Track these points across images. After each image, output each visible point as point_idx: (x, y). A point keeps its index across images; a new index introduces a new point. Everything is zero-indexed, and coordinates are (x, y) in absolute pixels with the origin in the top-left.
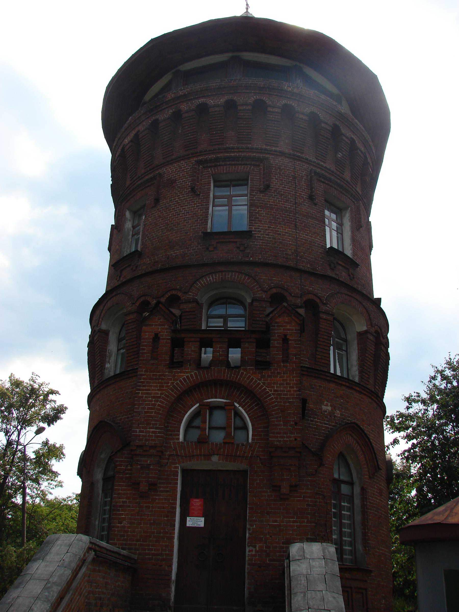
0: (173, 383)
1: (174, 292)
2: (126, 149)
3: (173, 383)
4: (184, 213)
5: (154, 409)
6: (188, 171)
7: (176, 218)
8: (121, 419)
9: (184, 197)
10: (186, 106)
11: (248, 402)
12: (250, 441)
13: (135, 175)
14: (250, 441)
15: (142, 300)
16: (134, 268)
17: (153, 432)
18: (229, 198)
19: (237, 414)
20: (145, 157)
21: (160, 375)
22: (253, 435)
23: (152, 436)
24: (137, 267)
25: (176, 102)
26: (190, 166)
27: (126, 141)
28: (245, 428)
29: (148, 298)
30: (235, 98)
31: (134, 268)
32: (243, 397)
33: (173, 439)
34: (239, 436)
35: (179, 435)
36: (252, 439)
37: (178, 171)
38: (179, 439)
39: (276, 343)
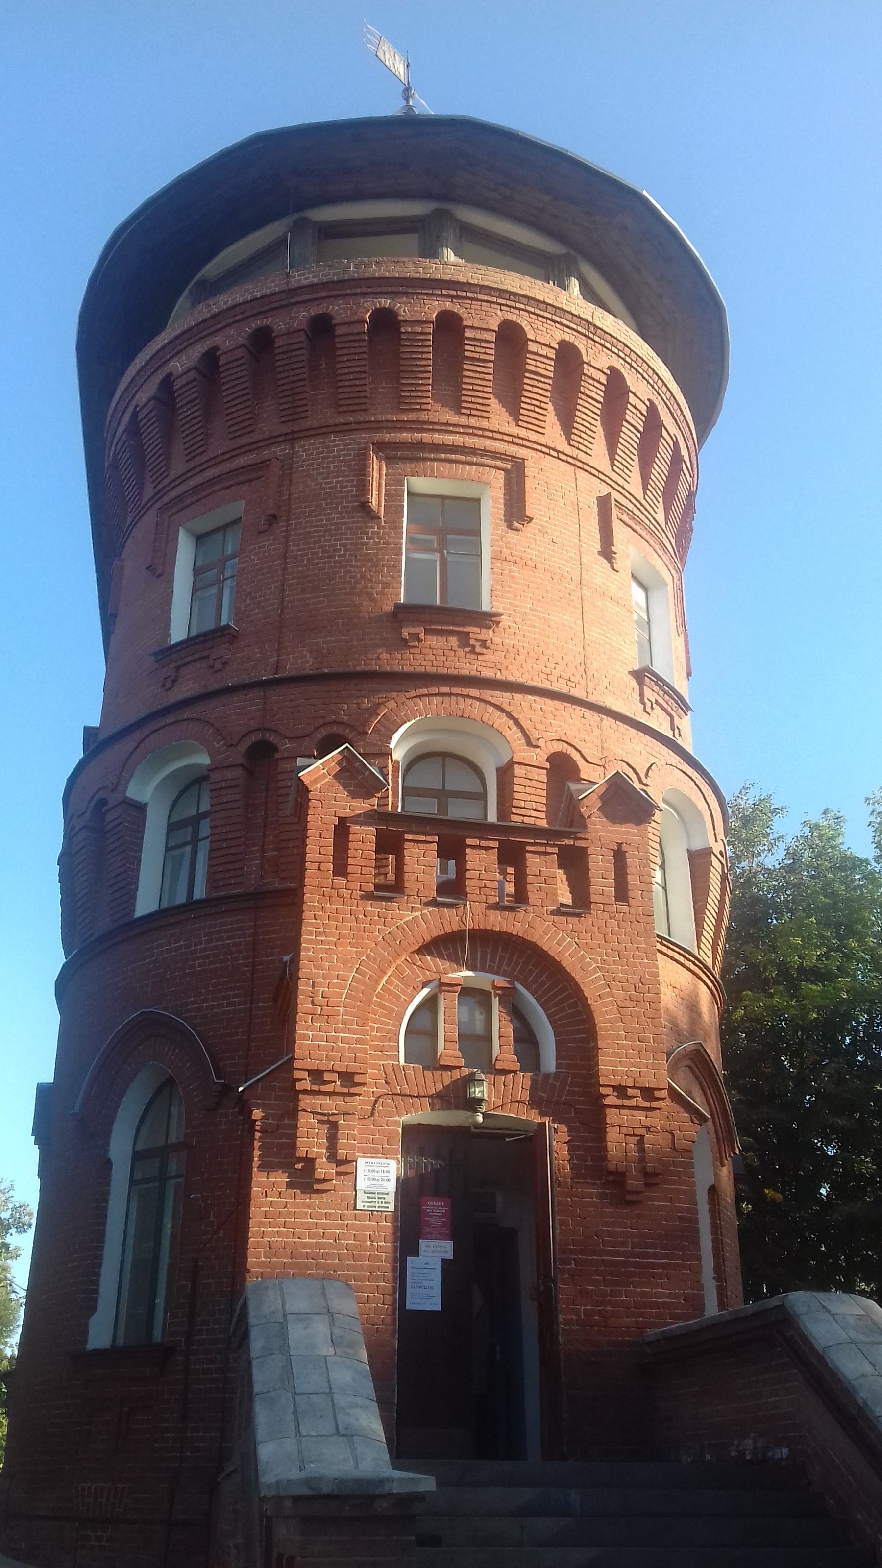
1: (335, 729)
2: (178, 384)
4: (344, 555)
6: (351, 460)
7: (324, 563)
8: (199, 1009)
9: (343, 518)
10: (345, 310)
11: (544, 983)
13: (201, 450)
15: (253, 739)
16: (218, 666)
20: (232, 413)
22: (558, 1058)
23: (342, 1050)
24: (225, 664)
25: (319, 295)
26: (353, 449)
27: (177, 366)
29: (272, 738)
30: (456, 309)
31: (218, 666)
32: (531, 971)
36: (558, 1066)
37: (324, 458)
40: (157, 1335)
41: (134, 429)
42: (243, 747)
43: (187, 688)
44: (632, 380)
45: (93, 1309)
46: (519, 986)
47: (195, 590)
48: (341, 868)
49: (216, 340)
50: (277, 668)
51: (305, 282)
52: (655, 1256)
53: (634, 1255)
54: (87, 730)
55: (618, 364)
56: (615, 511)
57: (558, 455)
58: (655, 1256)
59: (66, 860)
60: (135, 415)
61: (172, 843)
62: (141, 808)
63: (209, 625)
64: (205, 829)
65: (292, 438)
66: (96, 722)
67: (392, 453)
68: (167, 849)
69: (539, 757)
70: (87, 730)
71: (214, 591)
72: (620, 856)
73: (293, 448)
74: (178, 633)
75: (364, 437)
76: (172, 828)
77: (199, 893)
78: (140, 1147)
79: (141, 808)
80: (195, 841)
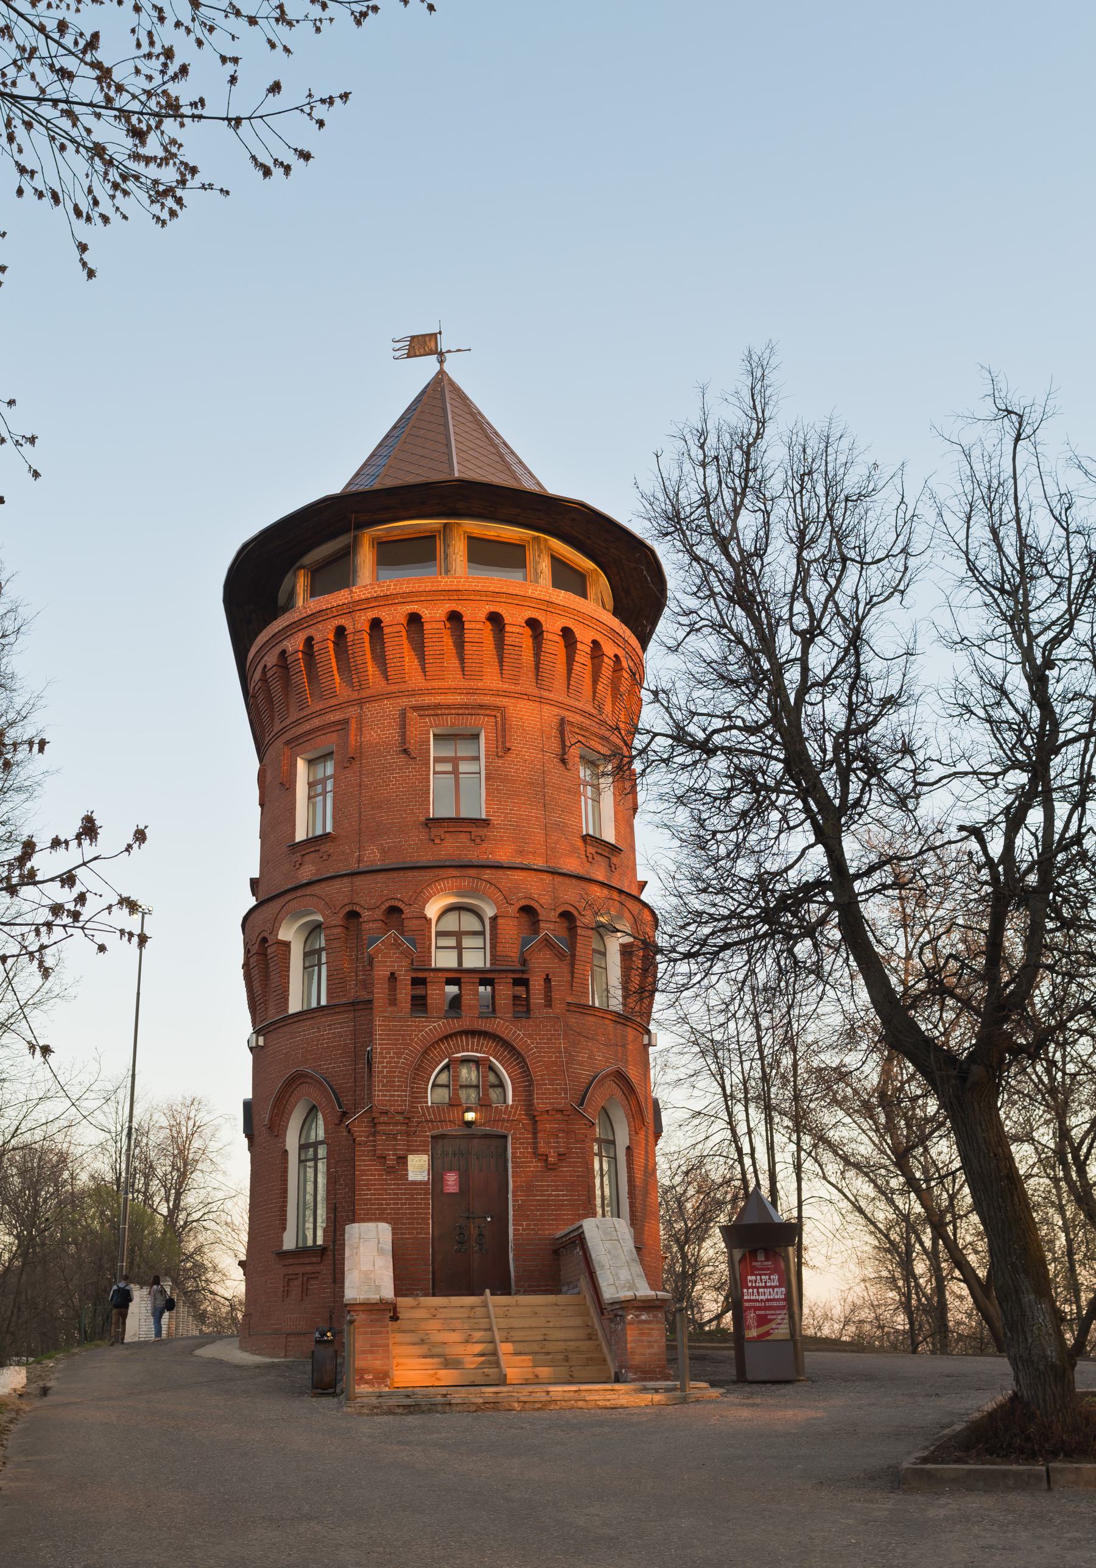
0: (416, 1035)
3: (416, 1035)
5: (396, 1067)
12: (510, 1102)
14: (510, 1102)
15: (348, 909)
16: (325, 857)
17: (398, 1096)
18: (455, 761)
19: (492, 1068)
21: (402, 1026)
28: (501, 1085)
29: (358, 909)
31: (325, 857)
33: (420, 1102)
34: (494, 1094)
35: (426, 1097)
38: (427, 1102)
39: (537, 984)
40: (320, 1242)
41: (264, 680)
42: (341, 915)
43: (307, 873)
44: (579, 633)
45: (284, 1229)
46: (492, 1059)
47: (310, 798)
48: (393, 1002)
49: (311, 632)
50: (359, 860)
51: (363, 597)
52: (563, 1195)
53: (551, 1195)
54: (251, 880)
55: (570, 624)
56: (567, 728)
57: (529, 697)
58: (563, 1195)
59: (246, 966)
60: (264, 672)
61: (307, 965)
62: (287, 945)
63: (319, 832)
64: (324, 960)
65: (361, 702)
66: (257, 875)
67: (422, 713)
68: (305, 968)
69: (512, 910)
70: (251, 880)
71: (321, 798)
72: (547, 980)
73: (361, 709)
74: (300, 836)
75: (405, 702)
76: (306, 955)
77: (323, 1002)
78: (302, 1142)
79: (287, 945)
80: (319, 965)
